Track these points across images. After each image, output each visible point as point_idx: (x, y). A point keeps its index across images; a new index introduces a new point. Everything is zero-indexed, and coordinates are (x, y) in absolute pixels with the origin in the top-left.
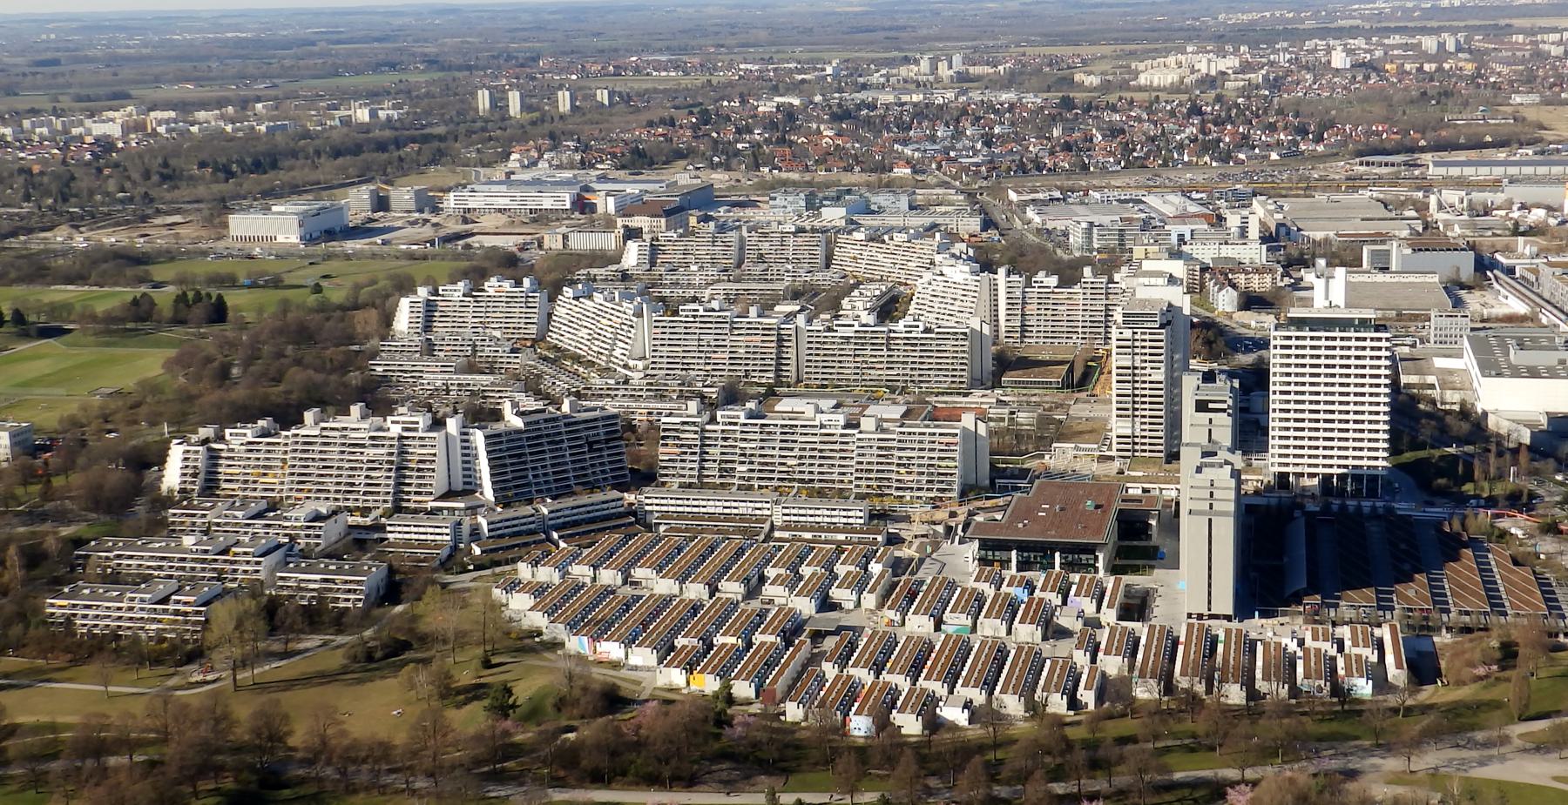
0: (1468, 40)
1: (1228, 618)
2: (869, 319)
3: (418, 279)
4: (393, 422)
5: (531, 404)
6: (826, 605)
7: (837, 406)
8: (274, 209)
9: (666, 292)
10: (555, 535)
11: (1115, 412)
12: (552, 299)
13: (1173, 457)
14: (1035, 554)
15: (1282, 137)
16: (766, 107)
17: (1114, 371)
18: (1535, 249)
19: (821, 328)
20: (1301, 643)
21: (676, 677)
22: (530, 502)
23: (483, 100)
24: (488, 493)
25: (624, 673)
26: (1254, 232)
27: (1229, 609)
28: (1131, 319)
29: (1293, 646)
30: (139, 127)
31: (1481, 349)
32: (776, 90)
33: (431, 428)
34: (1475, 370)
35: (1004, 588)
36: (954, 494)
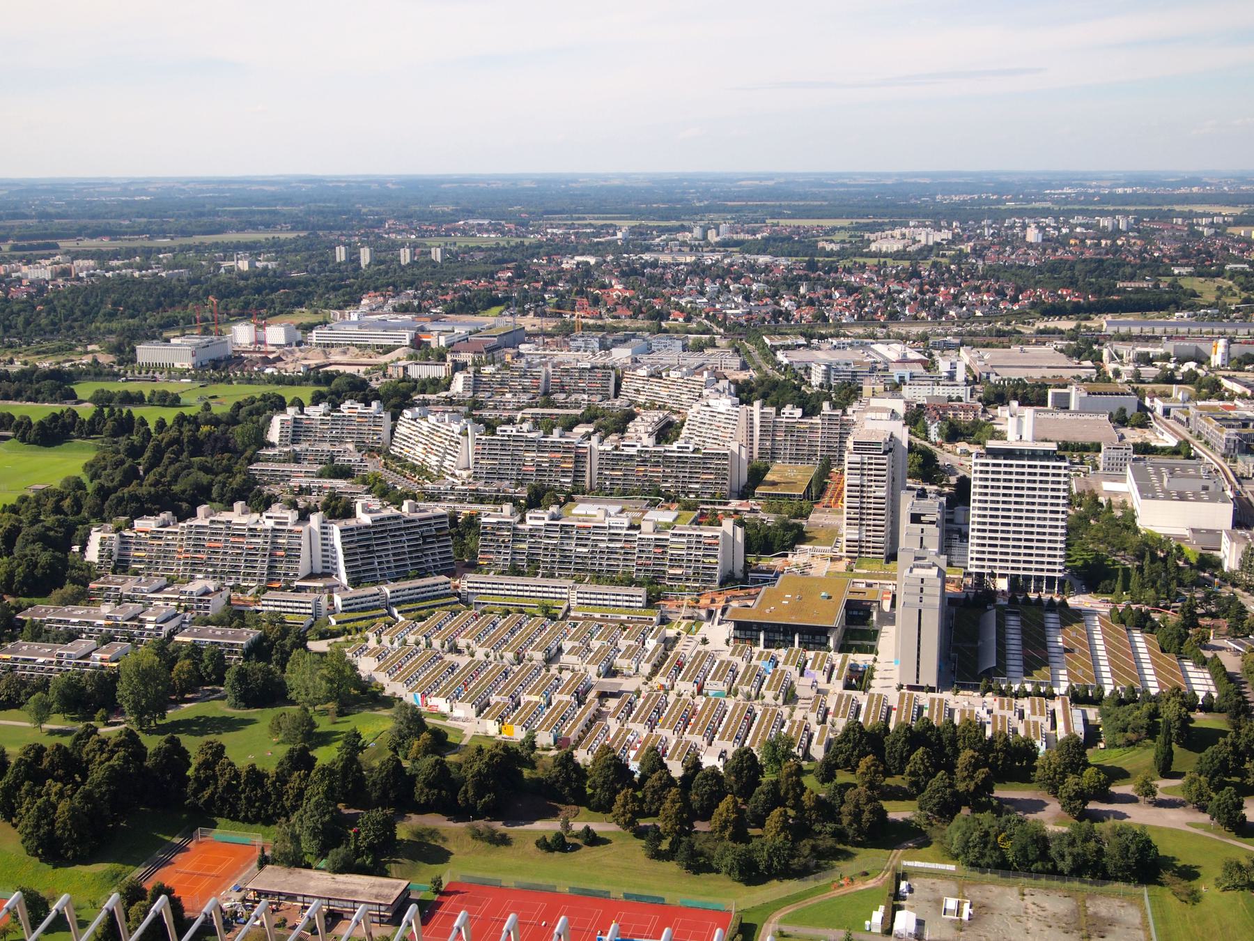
0: (1137, 221)
1: (932, 690)
2: (649, 442)
3: (288, 400)
4: (268, 517)
5: (376, 504)
6: (611, 672)
7: (622, 511)
8: (173, 341)
9: (486, 414)
10: (395, 611)
11: (845, 521)
12: (395, 418)
13: (892, 557)
14: (779, 634)
15: (985, 298)
16: (568, 264)
17: (846, 488)
18: (1187, 395)
19: (609, 448)
20: (989, 712)
21: (491, 727)
22: (376, 583)
23: (341, 254)
24: (343, 578)
25: (449, 723)
26: (961, 375)
27: (934, 684)
28: (860, 447)
29: (983, 714)
30: (65, 273)
31: (1141, 478)
32: (575, 251)
33: (298, 523)
34: (1135, 494)
35: (754, 662)
36: (716, 584)
